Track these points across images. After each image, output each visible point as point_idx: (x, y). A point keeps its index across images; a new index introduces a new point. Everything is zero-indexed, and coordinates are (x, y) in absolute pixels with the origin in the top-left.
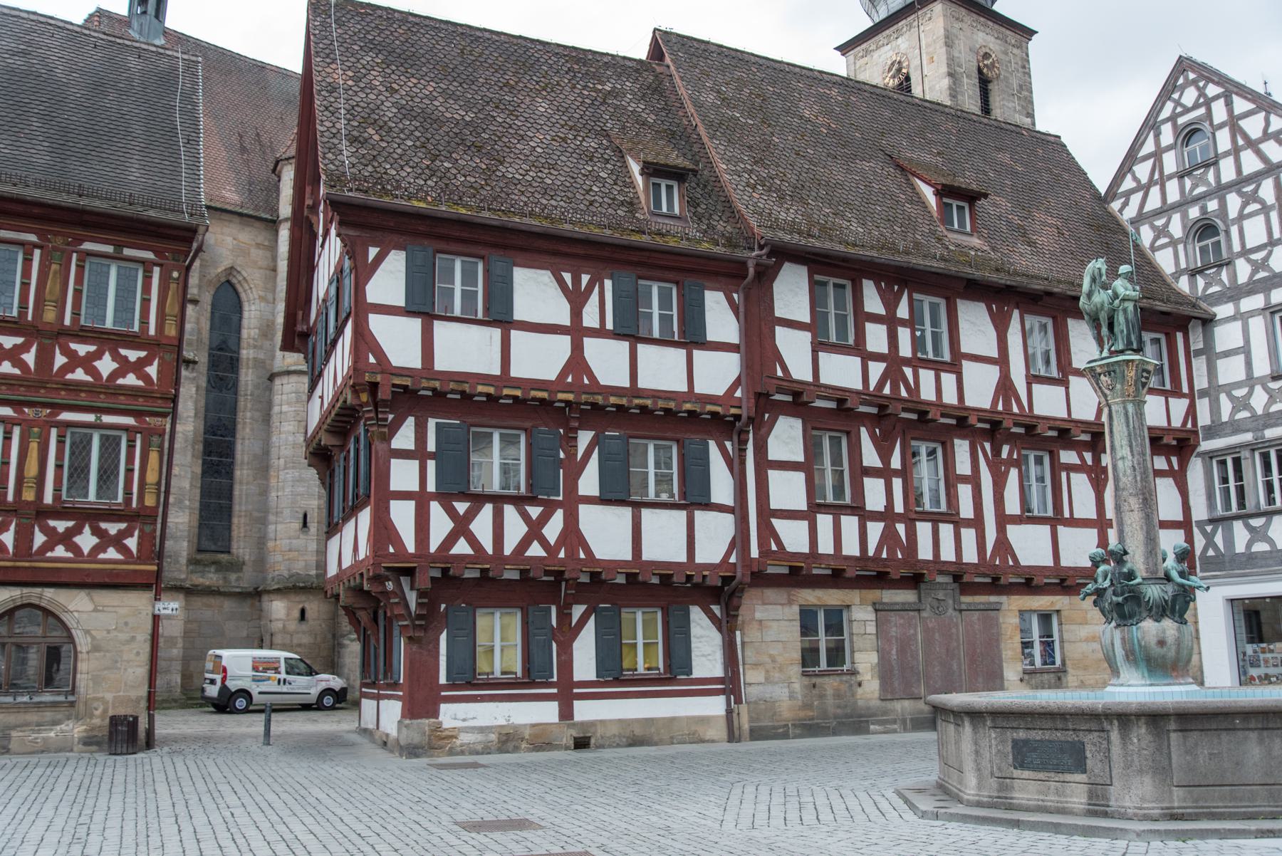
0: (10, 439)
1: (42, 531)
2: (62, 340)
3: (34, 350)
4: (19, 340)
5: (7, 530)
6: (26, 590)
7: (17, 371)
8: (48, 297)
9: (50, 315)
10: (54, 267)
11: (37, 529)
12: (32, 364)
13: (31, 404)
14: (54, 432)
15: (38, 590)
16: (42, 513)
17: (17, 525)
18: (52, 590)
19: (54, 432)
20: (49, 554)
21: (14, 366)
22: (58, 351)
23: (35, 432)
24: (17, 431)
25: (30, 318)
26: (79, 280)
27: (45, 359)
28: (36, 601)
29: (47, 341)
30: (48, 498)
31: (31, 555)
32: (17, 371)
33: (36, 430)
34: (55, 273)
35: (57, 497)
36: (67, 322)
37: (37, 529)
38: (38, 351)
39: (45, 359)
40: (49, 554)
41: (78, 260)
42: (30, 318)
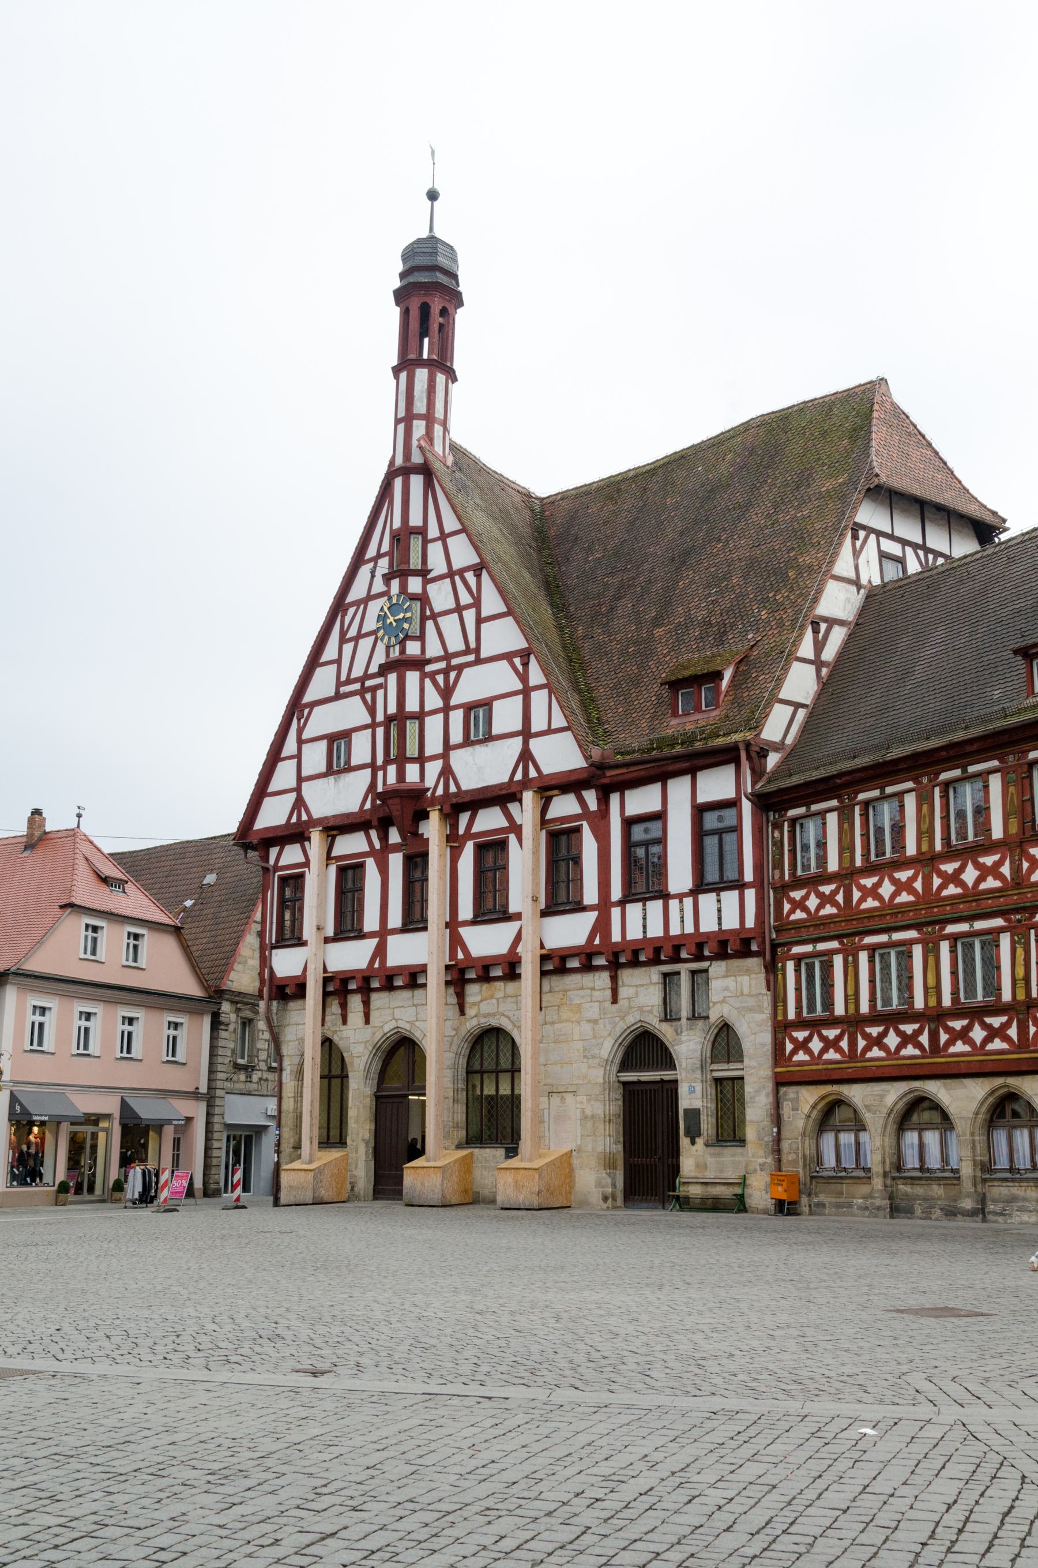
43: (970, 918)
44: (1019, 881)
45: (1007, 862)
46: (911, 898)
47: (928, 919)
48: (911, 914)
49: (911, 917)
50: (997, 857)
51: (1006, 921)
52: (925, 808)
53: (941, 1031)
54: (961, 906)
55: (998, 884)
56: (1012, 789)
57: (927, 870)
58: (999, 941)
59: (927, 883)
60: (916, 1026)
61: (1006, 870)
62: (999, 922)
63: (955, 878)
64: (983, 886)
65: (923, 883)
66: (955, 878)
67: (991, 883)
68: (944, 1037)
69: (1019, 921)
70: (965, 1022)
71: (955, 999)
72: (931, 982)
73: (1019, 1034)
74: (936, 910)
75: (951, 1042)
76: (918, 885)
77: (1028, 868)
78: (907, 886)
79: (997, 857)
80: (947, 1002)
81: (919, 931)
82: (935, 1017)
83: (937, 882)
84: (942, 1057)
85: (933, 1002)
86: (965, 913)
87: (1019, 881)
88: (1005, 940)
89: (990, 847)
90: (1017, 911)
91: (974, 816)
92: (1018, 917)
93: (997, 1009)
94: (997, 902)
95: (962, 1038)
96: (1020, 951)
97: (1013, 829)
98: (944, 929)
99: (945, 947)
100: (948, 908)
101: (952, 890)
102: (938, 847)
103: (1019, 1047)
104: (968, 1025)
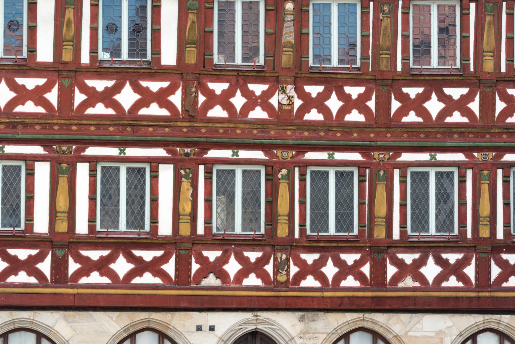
0: (465, 181)
1: (497, 264)
2: (500, 86)
3: (477, 98)
4: (464, 91)
5: (469, 264)
6: (487, 317)
7: (465, 120)
8: (486, 48)
9: (489, 66)
10: (488, 18)
11: (493, 262)
12: (477, 112)
13: (479, 149)
14: (500, 172)
15: (497, 317)
16: (496, 248)
17: (476, 259)
18: (508, 316)
19: (500, 172)
20: (504, 285)
21: (463, 115)
22: (497, 98)
23: (485, 173)
24: (469, 174)
25: (472, 69)
26: (510, 28)
27: (487, 105)
28: (494, 326)
29: (488, 90)
30: (500, 235)
31: (490, 286)
32: (465, 120)
33: (486, 172)
34: (490, 23)
35: (507, 233)
36: (503, 69)
37: (493, 262)
38: (481, 99)
39: (487, 105)
40: (504, 285)
41: (507, 8)
42: (472, 69)
43: (122, 144)
44: (192, 113)
45: (179, 93)
46: (41, 110)
47: (64, 137)
48: (38, 127)
49: (38, 132)
50: (165, 84)
51: (168, 152)
52: (70, 14)
53: (71, 260)
54: (111, 129)
55: (165, 112)
56: (192, 17)
57: (66, 83)
58: (157, 171)
59: (66, 97)
60: (34, 252)
61: (176, 99)
62: (160, 152)
63: (107, 97)
64: (143, 112)
65: (59, 96)
66: (107, 97)
67: (154, 110)
68: (73, 267)
69: (187, 155)
70: (105, 253)
71: (92, 228)
72: (62, 204)
73: (176, 270)
74: (74, 128)
75: (85, 271)
76: (52, 97)
77: (205, 103)
78: (38, 96)
79: (165, 84)
80: (82, 227)
81: (45, 148)
82: (62, 243)
83: (79, 98)
84: (72, 287)
85: (62, 227)
86: (118, 138)
87: (192, 113)
88: (166, 174)
89: (156, 71)
90: (186, 144)
91: (130, 34)
92: (187, 150)
93: (152, 241)
94: (160, 131)
95: (98, 270)
96: (186, 184)
97: (191, 58)
98: (84, 150)
99: (82, 170)
100: (93, 128)
101: (100, 109)
102: (85, 59)
103: (176, 283)
104: (109, 256)
